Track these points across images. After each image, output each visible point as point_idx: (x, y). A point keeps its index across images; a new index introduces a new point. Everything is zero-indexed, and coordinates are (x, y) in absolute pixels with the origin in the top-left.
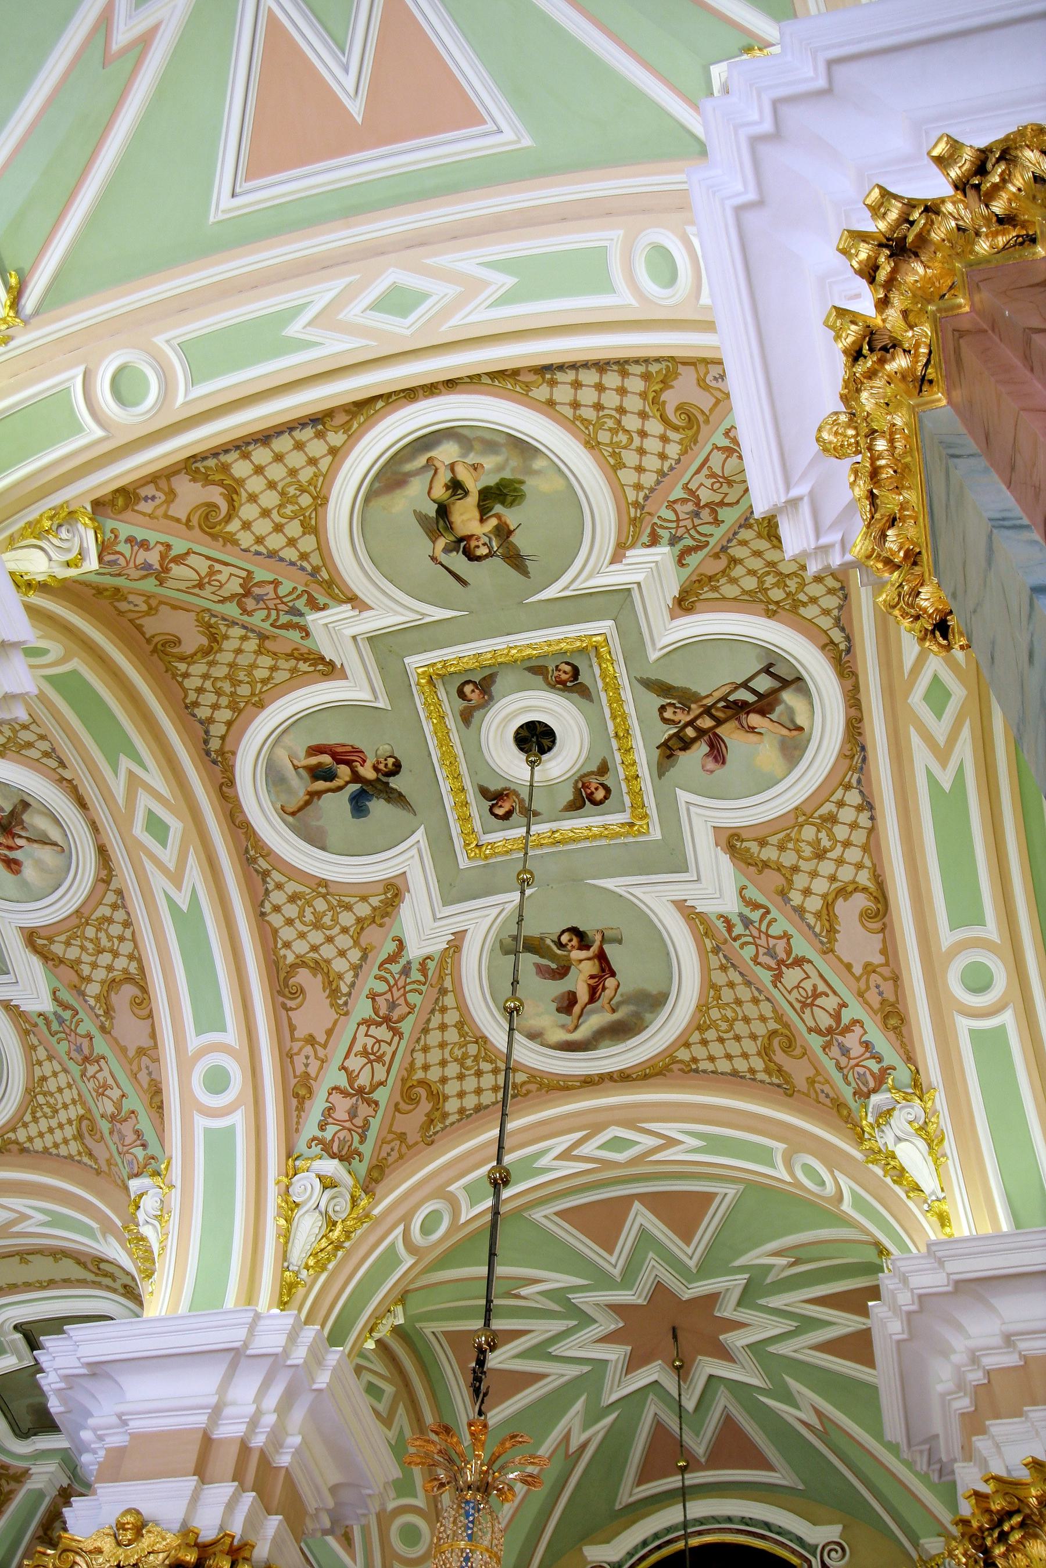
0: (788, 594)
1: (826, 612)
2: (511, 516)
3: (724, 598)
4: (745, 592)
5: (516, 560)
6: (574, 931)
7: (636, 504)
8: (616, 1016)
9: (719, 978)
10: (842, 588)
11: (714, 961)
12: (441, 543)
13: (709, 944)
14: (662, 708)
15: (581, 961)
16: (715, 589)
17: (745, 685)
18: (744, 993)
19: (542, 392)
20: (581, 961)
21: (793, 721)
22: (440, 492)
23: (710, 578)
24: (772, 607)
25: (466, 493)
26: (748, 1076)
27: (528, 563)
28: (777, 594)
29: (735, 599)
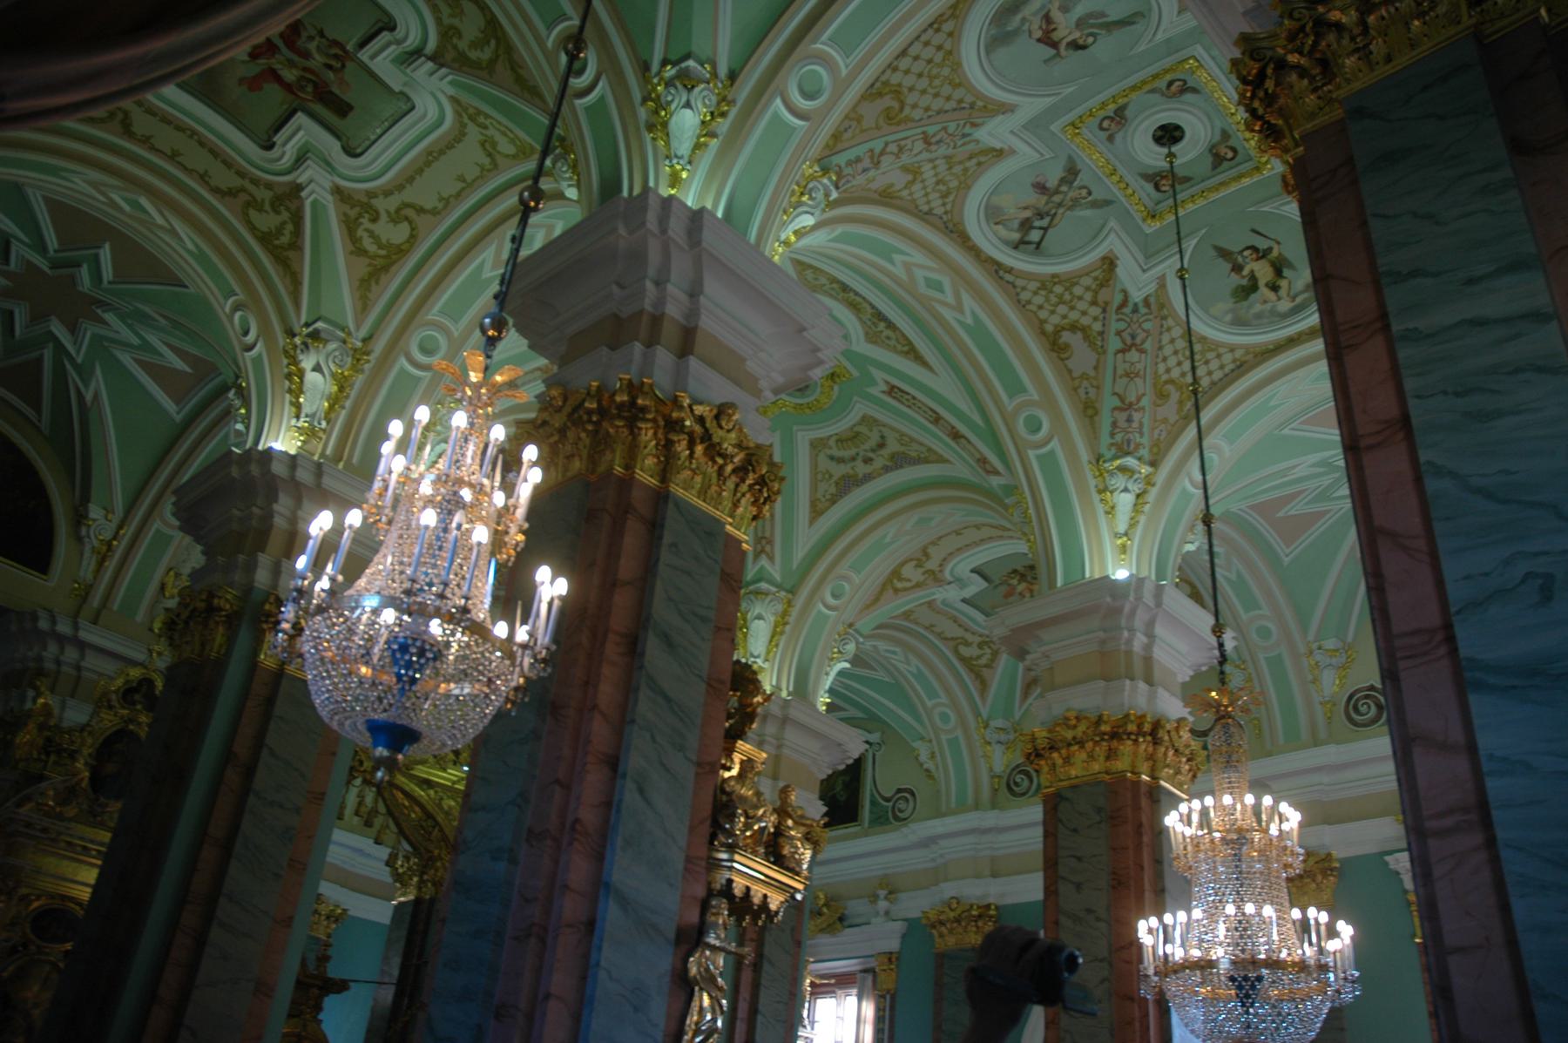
0: (1051, 292)
1: (1024, 289)
2: (1236, 280)
3: (1087, 274)
4: (1077, 283)
5: (1224, 253)
6: (1084, 47)
7: (1164, 318)
8: (1019, 17)
9: (958, 94)
10: (1024, 306)
11: (969, 99)
12: (1275, 253)
13: (980, 104)
14: (1090, 193)
15: (1070, 33)
16: (1096, 279)
17: (1045, 229)
18: (938, 104)
19: (1239, 354)
20: (1070, 33)
21: (1004, 225)
22: (1284, 283)
23: (1101, 286)
24: (1056, 280)
25: (1267, 285)
26: (895, 63)
27: (1215, 254)
28: (1058, 289)
29: (1081, 276)
